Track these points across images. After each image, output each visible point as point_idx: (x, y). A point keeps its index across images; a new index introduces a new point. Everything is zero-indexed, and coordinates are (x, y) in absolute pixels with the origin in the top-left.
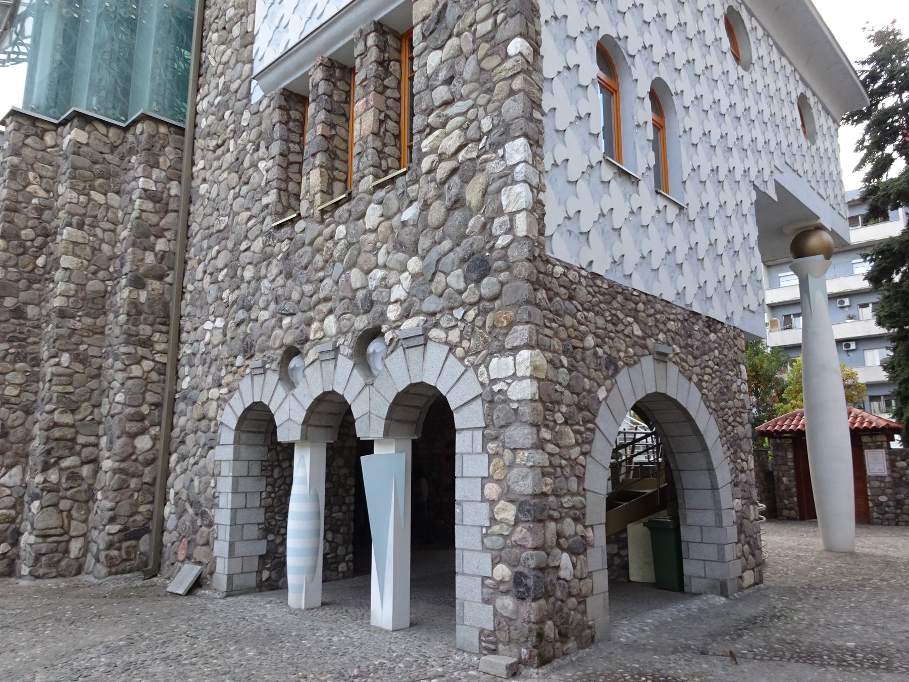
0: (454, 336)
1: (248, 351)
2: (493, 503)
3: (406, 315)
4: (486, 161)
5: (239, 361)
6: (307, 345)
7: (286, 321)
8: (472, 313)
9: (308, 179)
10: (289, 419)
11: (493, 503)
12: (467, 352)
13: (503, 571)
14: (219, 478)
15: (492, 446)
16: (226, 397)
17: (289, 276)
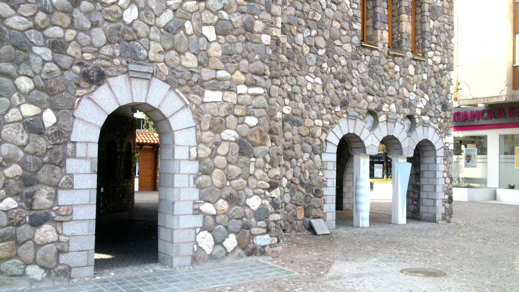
0: (437, 126)
1: (344, 104)
2: (445, 178)
3: (423, 114)
4: (446, 73)
5: (338, 109)
6: (381, 112)
7: (370, 98)
8: (442, 121)
9: (382, 33)
10: (372, 145)
11: (445, 178)
12: (440, 133)
13: (447, 197)
14: (325, 171)
15: (445, 162)
16: (329, 126)
17: (370, 75)
